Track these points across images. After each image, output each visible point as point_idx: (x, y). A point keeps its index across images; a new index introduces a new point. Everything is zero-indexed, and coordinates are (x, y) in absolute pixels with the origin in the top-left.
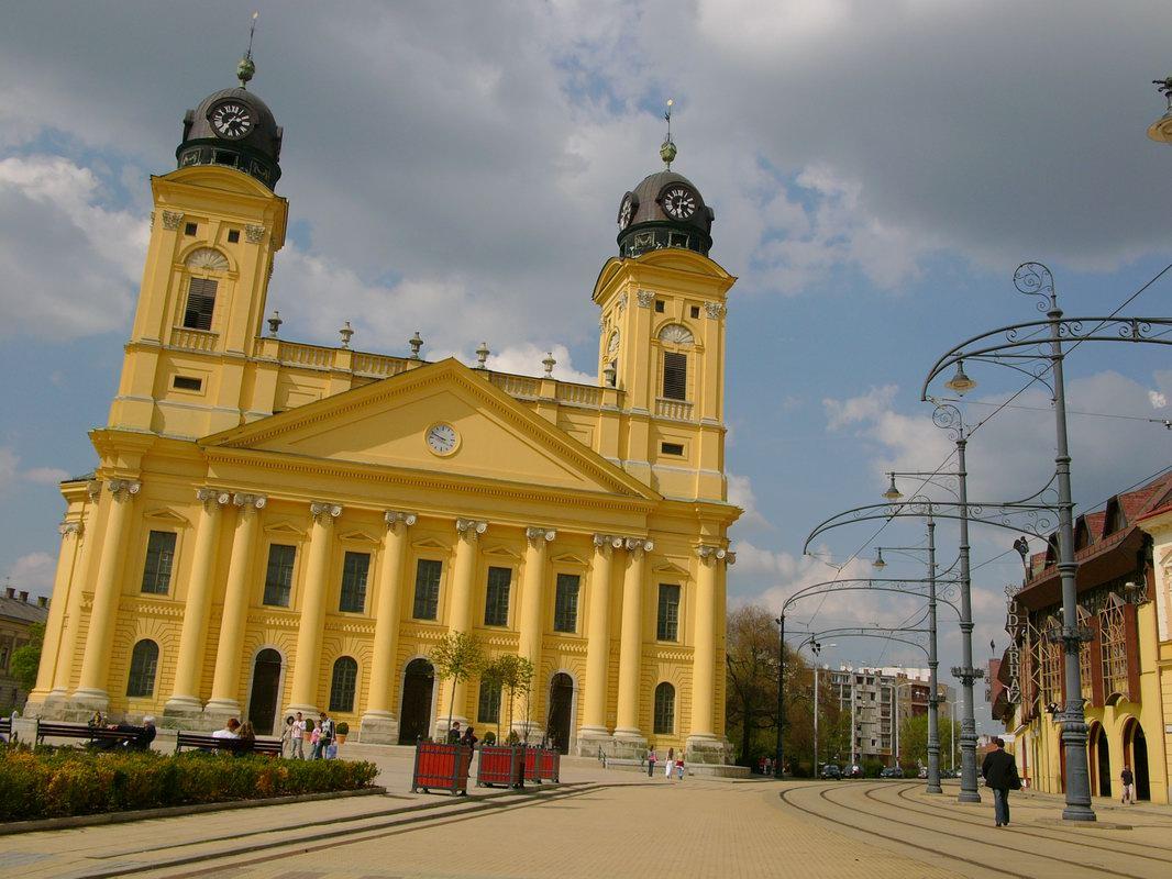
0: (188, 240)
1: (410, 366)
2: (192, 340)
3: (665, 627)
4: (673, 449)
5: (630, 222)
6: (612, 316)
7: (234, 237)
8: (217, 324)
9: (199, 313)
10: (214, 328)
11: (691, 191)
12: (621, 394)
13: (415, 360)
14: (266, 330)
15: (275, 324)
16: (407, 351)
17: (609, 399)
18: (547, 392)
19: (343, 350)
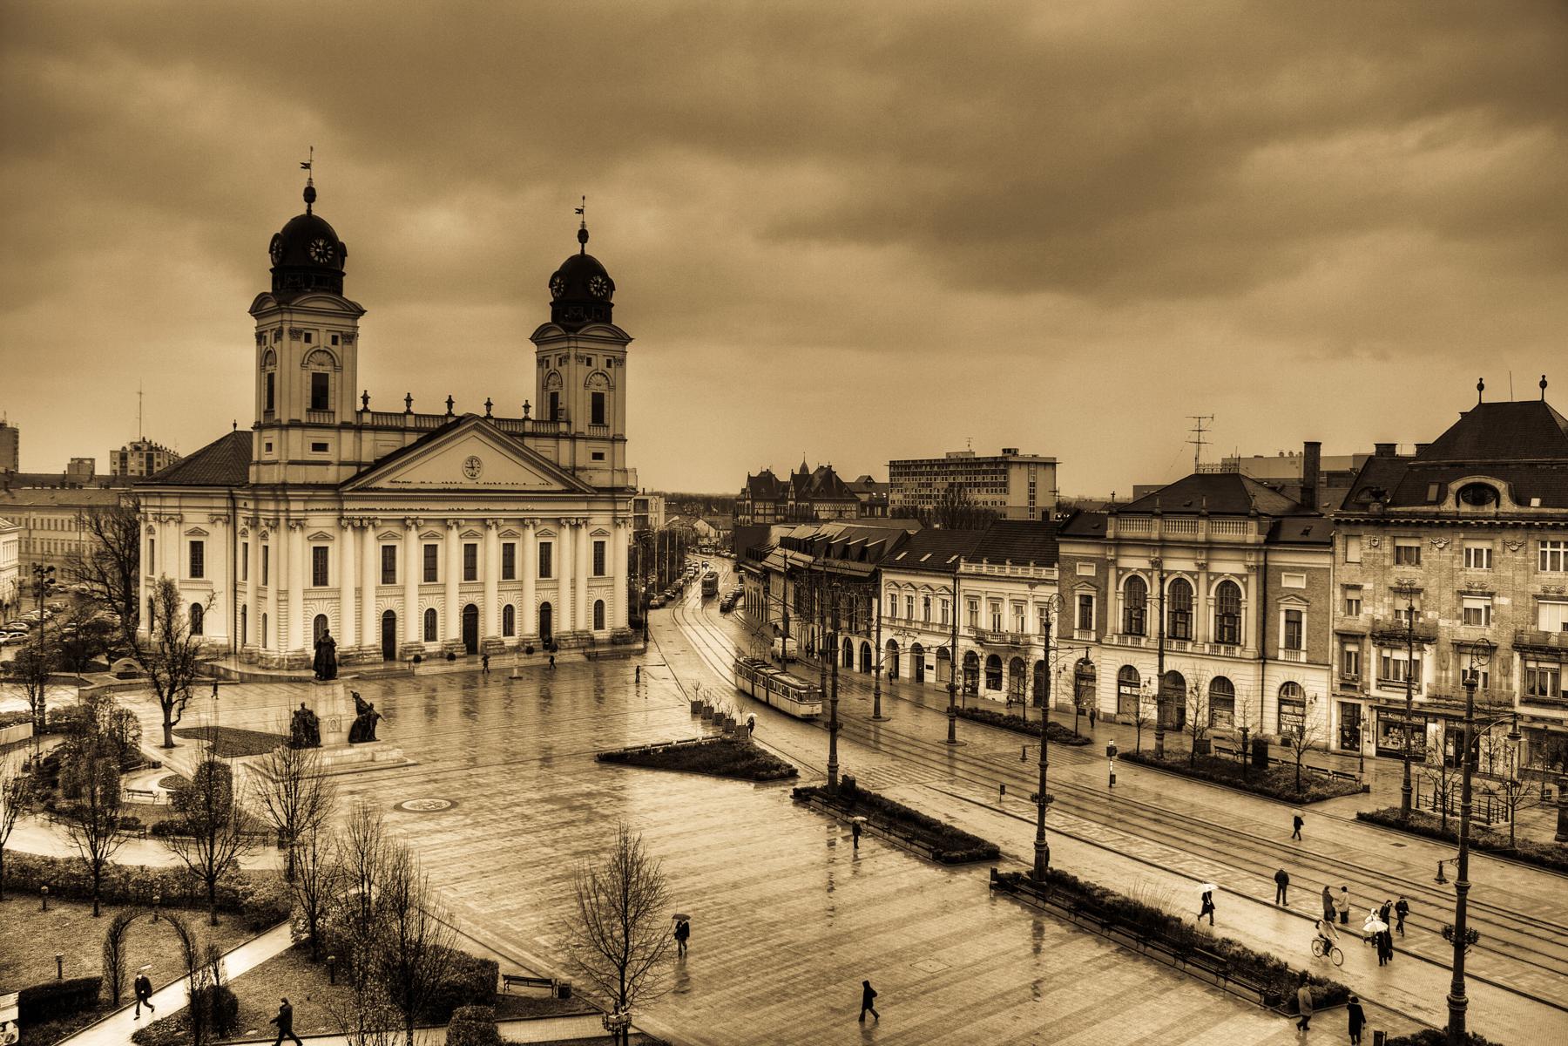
0: (308, 346)
1: (450, 420)
2: (318, 418)
3: (599, 568)
4: (598, 456)
5: (564, 294)
6: (552, 360)
7: (335, 341)
8: (333, 402)
9: (320, 396)
10: (331, 407)
11: (604, 274)
12: (569, 423)
13: (450, 414)
14: (360, 406)
15: (365, 399)
16: (444, 411)
17: (563, 427)
18: (528, 426)
19: (409, 412)
